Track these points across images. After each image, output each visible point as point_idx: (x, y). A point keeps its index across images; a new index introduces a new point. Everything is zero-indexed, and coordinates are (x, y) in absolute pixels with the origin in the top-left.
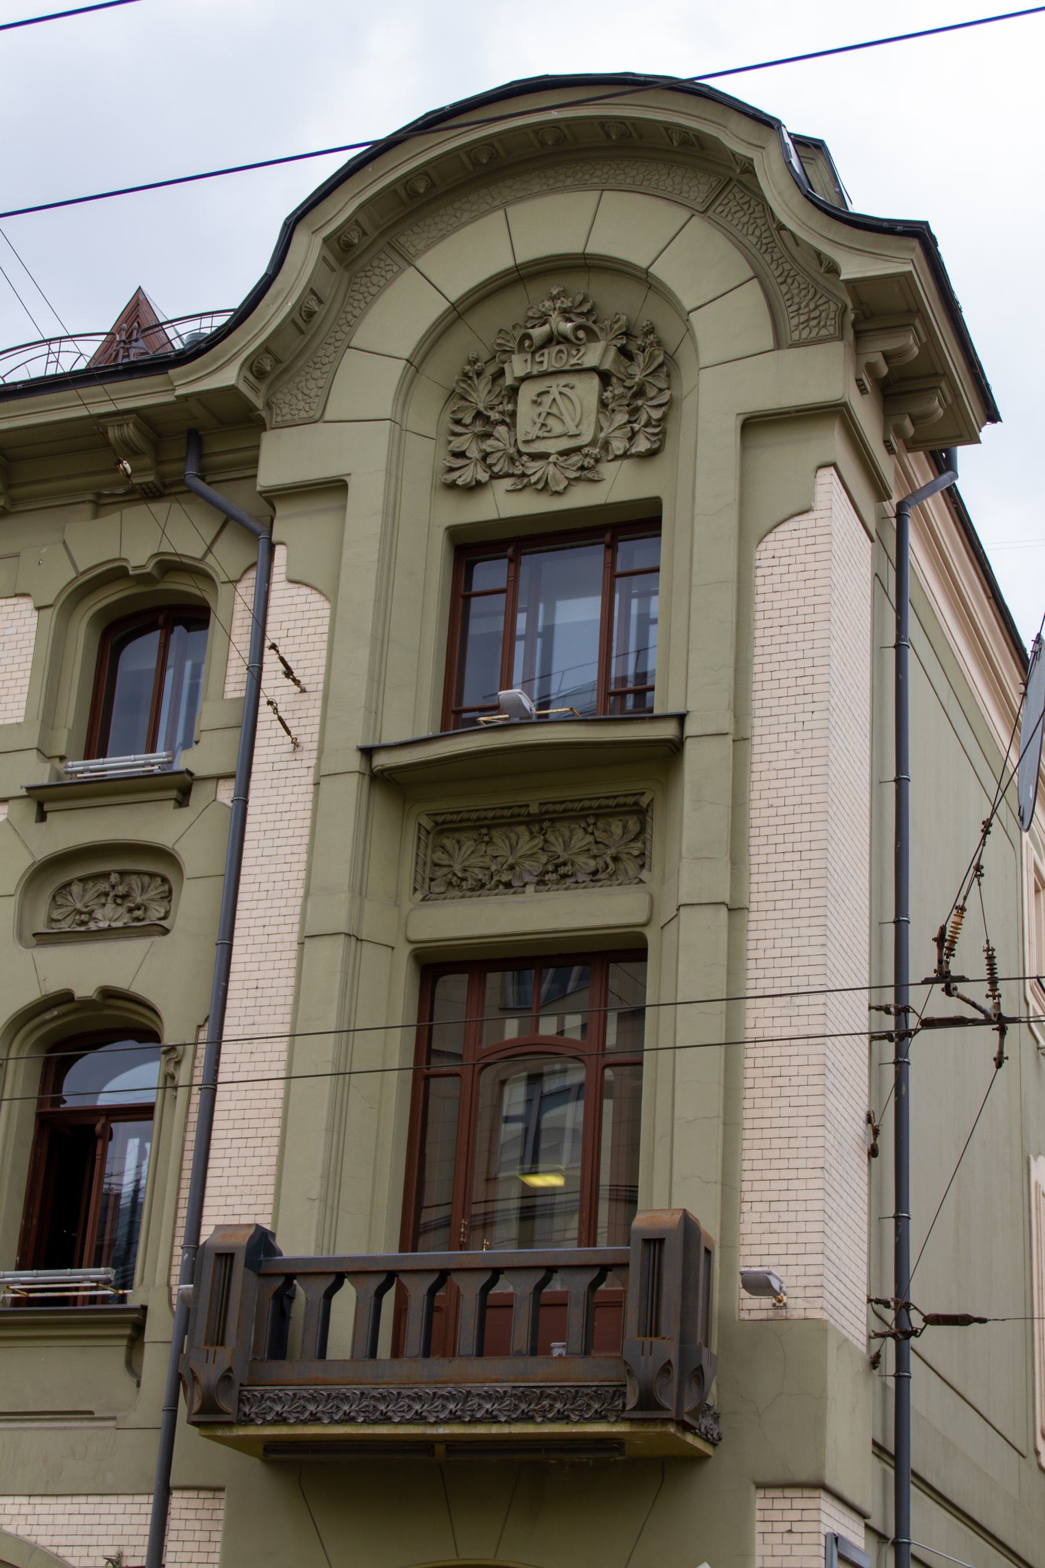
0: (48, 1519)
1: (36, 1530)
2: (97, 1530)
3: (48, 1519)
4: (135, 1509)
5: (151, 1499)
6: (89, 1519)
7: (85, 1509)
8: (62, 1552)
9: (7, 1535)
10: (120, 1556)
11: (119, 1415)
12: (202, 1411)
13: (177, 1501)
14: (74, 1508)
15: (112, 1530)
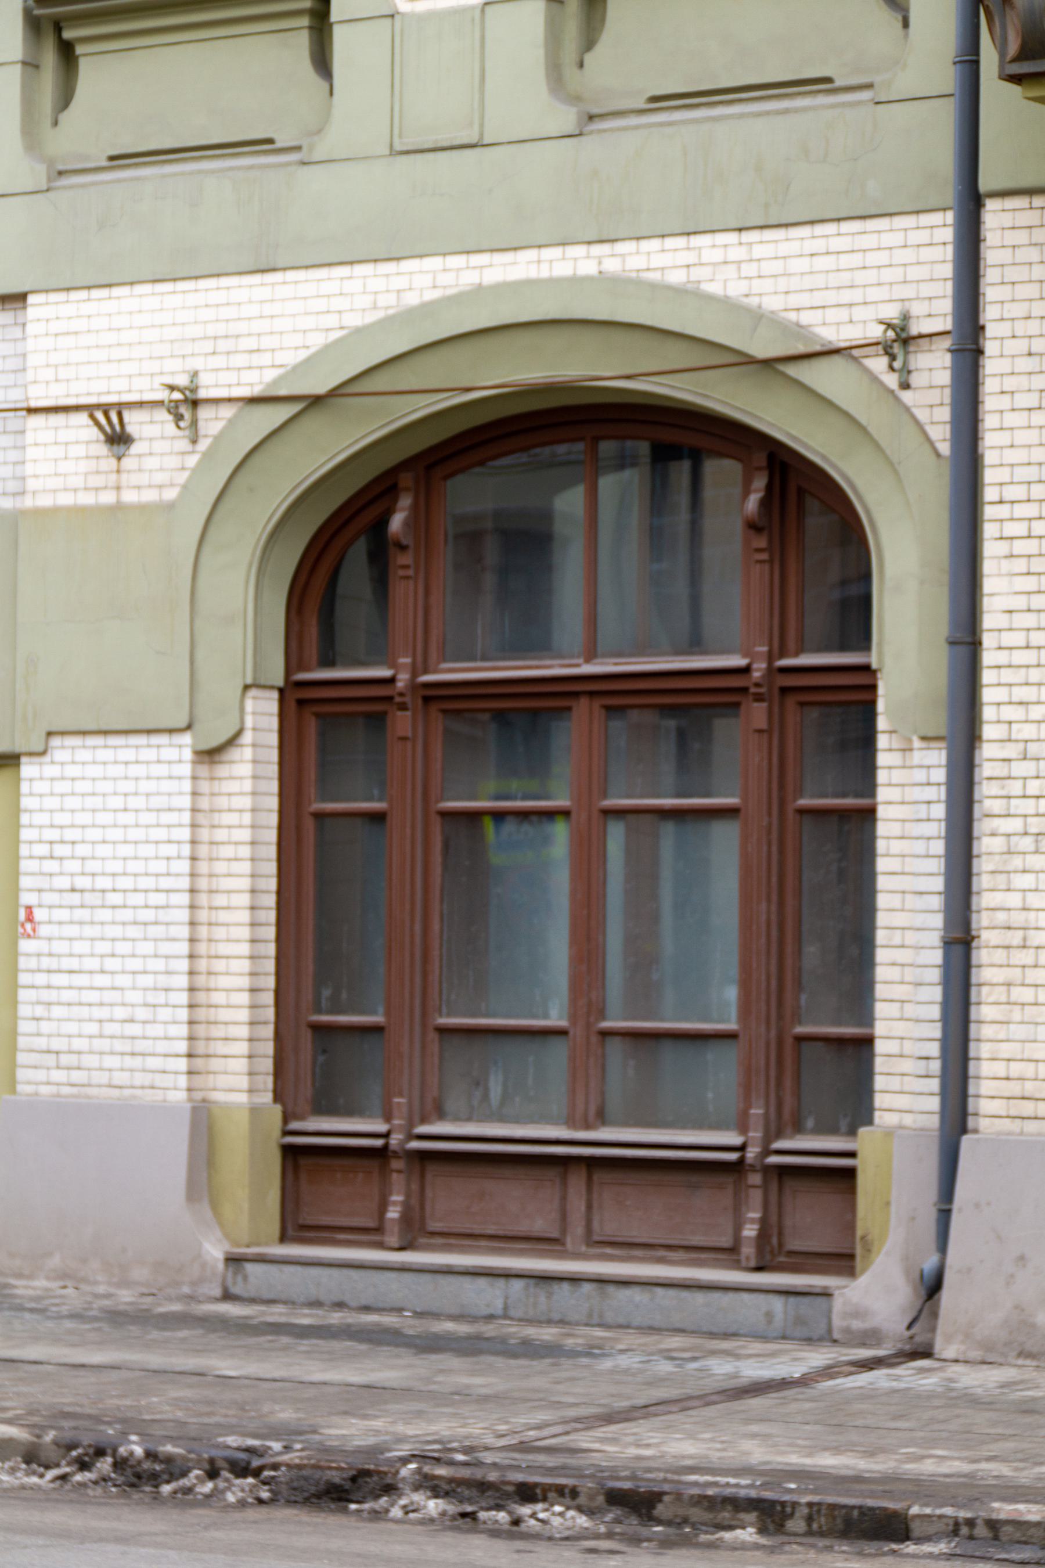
0: (777, 267)
1: (757, 286)
2: (861, 277)
3: (777, 267)
4: (923, 236)
5: (950, 217)
6: (845, 261)
7: (836, 244)
8: (805, 318)
9: (710, 298)
10: (906, 317)
11: (877, 79)
12: (1023, 55)
13: (995, 216)
14: (819, 245)
15: (887, 275)
